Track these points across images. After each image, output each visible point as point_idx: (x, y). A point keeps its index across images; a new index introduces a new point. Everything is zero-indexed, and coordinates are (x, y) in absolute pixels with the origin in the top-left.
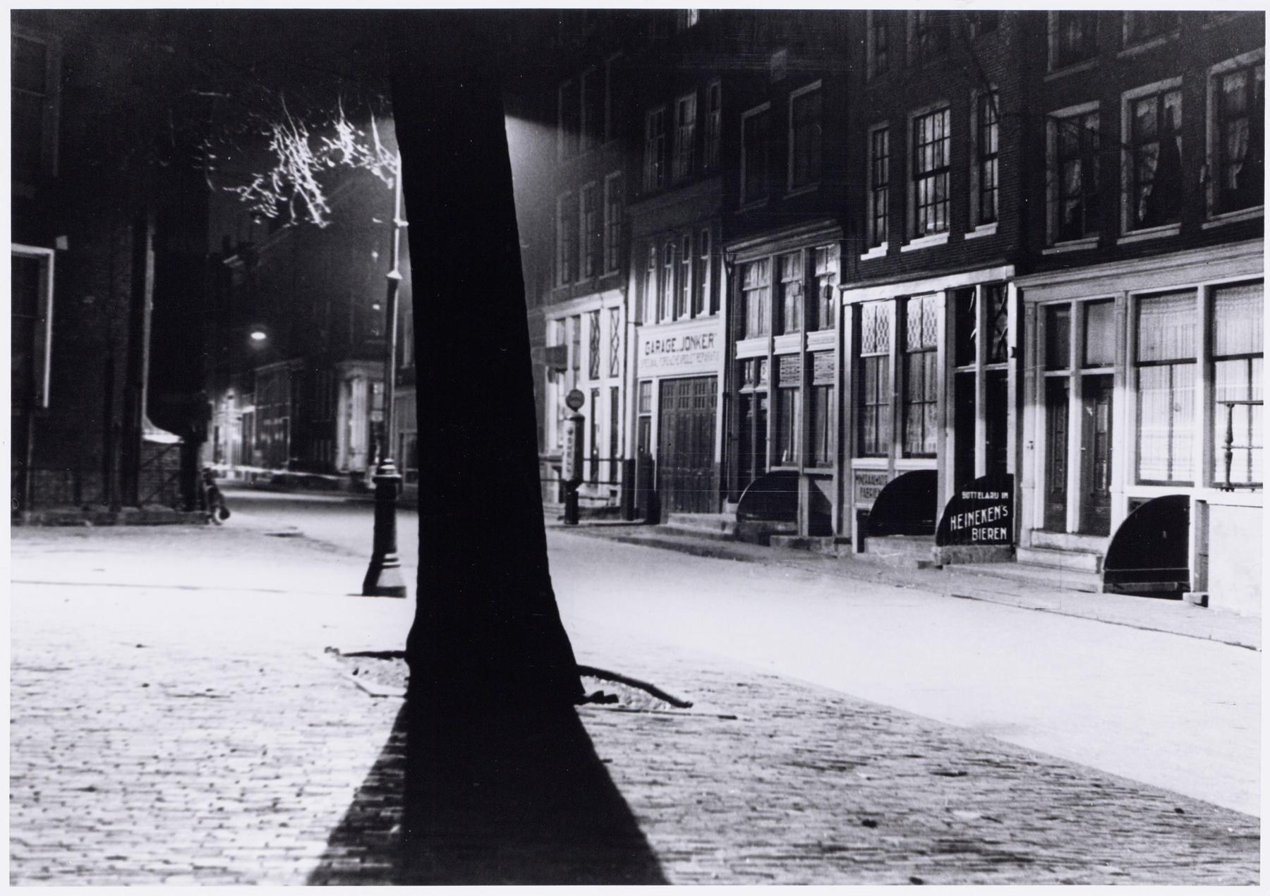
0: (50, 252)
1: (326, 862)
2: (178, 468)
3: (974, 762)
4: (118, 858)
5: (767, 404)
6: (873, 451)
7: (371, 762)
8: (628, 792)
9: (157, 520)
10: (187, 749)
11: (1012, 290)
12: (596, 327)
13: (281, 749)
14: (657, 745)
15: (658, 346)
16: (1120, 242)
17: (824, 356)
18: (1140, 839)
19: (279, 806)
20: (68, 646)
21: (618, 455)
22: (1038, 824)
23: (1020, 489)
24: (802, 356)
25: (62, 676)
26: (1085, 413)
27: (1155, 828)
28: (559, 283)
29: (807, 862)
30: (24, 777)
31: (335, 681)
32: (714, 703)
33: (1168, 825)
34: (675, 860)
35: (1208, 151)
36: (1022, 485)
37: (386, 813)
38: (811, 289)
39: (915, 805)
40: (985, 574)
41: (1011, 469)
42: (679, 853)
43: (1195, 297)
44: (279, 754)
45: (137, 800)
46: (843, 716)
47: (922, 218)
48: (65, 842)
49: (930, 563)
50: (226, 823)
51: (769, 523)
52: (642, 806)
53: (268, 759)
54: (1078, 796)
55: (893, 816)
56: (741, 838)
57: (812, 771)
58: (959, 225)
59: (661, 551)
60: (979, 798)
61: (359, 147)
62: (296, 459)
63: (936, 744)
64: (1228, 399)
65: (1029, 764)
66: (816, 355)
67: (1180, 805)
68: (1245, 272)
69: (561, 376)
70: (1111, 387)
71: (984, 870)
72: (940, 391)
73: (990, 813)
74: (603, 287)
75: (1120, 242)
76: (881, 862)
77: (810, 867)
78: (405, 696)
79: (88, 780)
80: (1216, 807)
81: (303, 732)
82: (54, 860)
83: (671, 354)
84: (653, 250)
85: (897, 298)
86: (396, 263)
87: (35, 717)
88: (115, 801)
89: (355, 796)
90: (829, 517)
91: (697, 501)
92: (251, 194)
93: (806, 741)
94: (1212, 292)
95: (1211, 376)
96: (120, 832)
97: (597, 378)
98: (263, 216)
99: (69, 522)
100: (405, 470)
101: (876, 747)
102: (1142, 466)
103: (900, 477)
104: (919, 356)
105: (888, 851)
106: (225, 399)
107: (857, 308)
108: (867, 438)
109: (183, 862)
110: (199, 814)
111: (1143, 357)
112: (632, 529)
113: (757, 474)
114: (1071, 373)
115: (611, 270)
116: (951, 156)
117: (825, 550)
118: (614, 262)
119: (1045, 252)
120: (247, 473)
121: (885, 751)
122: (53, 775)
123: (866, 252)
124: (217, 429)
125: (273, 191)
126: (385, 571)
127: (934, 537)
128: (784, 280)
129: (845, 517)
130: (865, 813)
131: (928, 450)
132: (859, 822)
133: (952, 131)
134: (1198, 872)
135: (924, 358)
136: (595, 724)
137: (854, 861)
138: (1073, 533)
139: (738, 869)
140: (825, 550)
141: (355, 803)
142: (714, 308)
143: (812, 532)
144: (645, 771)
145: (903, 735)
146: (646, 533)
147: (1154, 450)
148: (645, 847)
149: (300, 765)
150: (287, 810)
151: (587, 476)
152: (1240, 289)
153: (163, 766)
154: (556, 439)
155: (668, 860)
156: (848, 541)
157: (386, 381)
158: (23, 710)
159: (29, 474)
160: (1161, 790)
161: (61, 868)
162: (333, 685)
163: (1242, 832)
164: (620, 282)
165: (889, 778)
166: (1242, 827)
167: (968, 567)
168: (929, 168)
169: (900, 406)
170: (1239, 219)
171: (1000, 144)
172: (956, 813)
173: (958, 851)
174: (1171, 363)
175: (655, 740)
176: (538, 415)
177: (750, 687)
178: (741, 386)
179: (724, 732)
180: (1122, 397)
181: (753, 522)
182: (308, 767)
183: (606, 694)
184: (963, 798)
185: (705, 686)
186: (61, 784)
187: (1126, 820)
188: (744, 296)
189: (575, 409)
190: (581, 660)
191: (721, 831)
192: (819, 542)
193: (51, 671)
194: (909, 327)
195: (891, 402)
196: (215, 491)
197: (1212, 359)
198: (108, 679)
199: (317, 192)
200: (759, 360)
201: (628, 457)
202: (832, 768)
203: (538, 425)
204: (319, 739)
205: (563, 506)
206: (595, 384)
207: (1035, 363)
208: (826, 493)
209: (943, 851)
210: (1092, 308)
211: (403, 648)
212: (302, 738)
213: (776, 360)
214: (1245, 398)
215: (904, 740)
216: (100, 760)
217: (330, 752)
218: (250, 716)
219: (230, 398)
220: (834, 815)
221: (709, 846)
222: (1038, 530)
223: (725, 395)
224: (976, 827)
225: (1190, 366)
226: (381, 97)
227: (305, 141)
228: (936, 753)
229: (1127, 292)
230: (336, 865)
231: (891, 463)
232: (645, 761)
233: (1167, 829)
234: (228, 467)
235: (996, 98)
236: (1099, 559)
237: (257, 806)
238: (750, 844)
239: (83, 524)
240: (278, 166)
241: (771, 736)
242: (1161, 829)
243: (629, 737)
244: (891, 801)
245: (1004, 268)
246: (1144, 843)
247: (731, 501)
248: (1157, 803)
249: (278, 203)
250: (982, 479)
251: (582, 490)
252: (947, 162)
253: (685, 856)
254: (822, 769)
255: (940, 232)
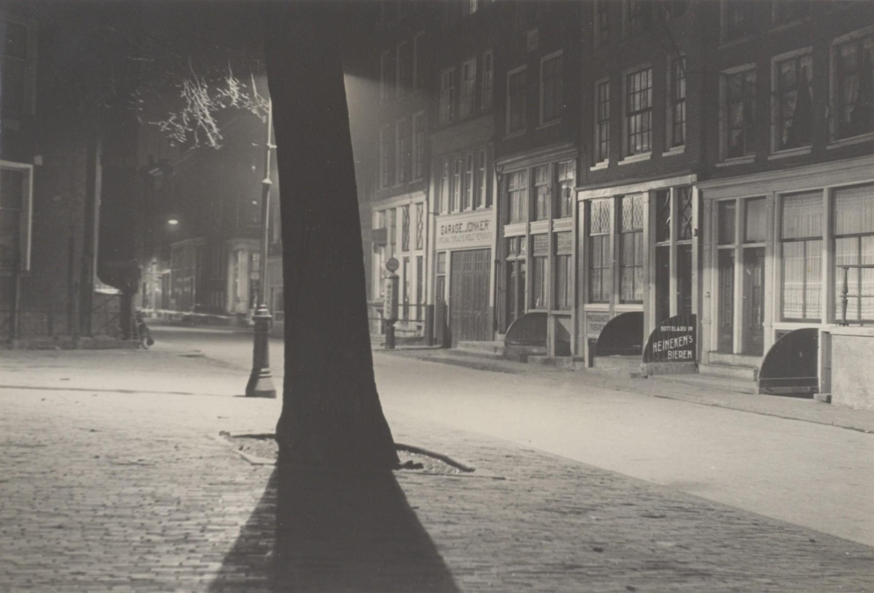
0: (30, 166)
1: (221, 576)
2: (118, 311)
3: (671, 509)
4: (79, 573)
5: (525, 267)
6: (599, 299)
7: (252, 509)
8: (431, 528)
9: (104, 346)
10: (125, 500)
11: (695, 191)
12: (406, 216)
13: (190, 500)
14: (451, 497)
15: (450, 229)
16: (770, 158)
17: (564, 235)
18: (785, 560)
19: (189, 538)
20: (44, 430)
21: (423, 302)
22: (715, 550)
23: (701, 325)
24: (549, 236)
25: (41, 451)
26: (745, 273)
27: (795, 553)
28: (381, 187)
29: (554, 575)
30: (14, 518)
31: (227, 454)
32: (490, 469)
33: (805, 550)
34: (463, 574)
35: (831, 97)
36: (703, 322)
37: (263, 543)
38: (556, 191)
39: (630, 537)
40: (677, 381)
41: (694, 311)
42: (465, 569)
43: (822, 196)
44: (188, 503)
45: (91, 535)
46: (579, 477)
47: (633, 142)
48: (43, 562)
49: (639, 374)
50: (153, 550)
51: (527, 347)
52: (441, 538)
53: (181, 507)
54: (742, 531)
55: (614, 544)
56: (509, 559)
57: (557, 515)
58: (658, 147)
59: (452, 366)
60: (674, 533)
61: (243, 95)
62: (199, 305)
63: (644, 496)
64: (844, 264)
65: (709, 510)
66: (559, 235)
67: (813, 537)
68: (857, 179)
69: (383, 249)
70: (763, 256)
71: (678, 582)
72: (645, 259)
73: (681, 543)
74: (412, 189)
75: (770, 158)
76: (606, 576)
77: (557, 579)
78: (276, 464)
79: (58, 521)
80: (838, 538)
81: (205, 489)
82: (35, 575)
83: (459, 234)
84: (447, 164)
85: (615, 196)
86: (268, 173)
87: (22, 478)
88: (77, 535)
89: (241, 532)
90: (569, 344)
91: (477, 331)
92: (168, 126)
93: (553, 494)
94: (833, 192)
95: (832, 249)
96: (80, 556)
97: (408, 250)
98: (176, 141)
99: (44, 347)
100: (275, 312)
101: (602, 498)
102: (848, 310)
103: (618, 317)
104: (630, 235)
105: (611, 568)
106: (150, 265)
107: (588, 203)
108: (595, 290)
109: (123, 576)
110: (134, 544)
111: (786, 236)
112: (431, 352)
113: (519, 315)
114: (736, 247)
115: (417, 178)
116: (653, 100)
117: (566, 366)
118: (419, 173)
119: (718, 165)
120: (165, 314)
121: (609, 501)
122: (34, 517)
123: (594, 165)
124: (145, 285)
125: (183, 124)
126: (261, 380)
127: (642, 357)
128: (537, 184)
129: (580, 343)
130: (596, 543)
131: (637, 298)
132: (591, 549)
133: (653, 83)
134: (825, 582)
135: (634, 236)
136: (407, 483)
137: (588, 575)
138: (738, 354)
139: (507, 580)
140: (566, 366)
141: (241, 537)
142: (489, 203)
143: (557, 353)
144: (442, 514)
145: (621, 490)
146: (442, 354)
147: (793, 297)
148: (443, 565)
149: (203, 511)
150: (195, 541)
151: (401, 316)
152: (853, 190)
153: (108, 512)
154: (379, 291)
155: (458, 574)
156: (582, 360)
157: (261, 252)
158: (14, 474)
159: (17, 315)
160: (799, 527)
161: (39, 580)
162: (225, 457)
163: (855, 555)
164: (423, 186)
165: (612, 519)
166: (855, 551)
167: (666, 377)
168: (638, 108)
169: (617, 268)
170: (852, 143)
171: (687, 92)
172: (659, 543)
173: (660, 568)
174: (805, 240)
175: (448, 493)
176: (366, 275)
177: (514, 457)
178: (508, 256)
179: (496, 488)
180: (771, 264)
181: (516, 348)
182: (209, 512)
183: (414, 463)
184: (662, 533)
185: (484, 457)
186: (40, 523)
187: (776, 548)
188: (510, 195)
189: (393, 271)
190: (397, 440)
191: (495, 555)
192: (562, 360)
193: (33, 447)
194: (624, 215)
195: (611, 266)
196: (143, 327)
197: (833, 237)
198: (71, 452)
199: (214, 125)
200: (521, 237)
201: (429, 303)
202: (571, 512)
203: (367, 281)
204: (216, 494)
205: (384, 336)
206: (406, 254)
207: (711, 240)
208: (567, 328)
209: (649, 569)
210: (750, 203)
211: (274, 432)
212: (204, 493)
213: (532, 238)
214: (857, 264)
215: (622, 493)
216: (66, 507)
217: (223, 502)
218: (168, 478)
219: (154, 263)
220: (573, 544)
221: (487, 564)
222: (714, 352)
223: (497, 262)
224: (673, 552)
225: (818, 242)
226: (258, 61)
227: (205, 90)
228: (644, 502)
229: (774, 192)
230: (229, 578)
231: (612, 307)
232: (442, 508)
233: (804, 553)
234: (152, 310)
235: (684, 61)
236: (756, 372)
237: (173, 538)
238: (515, 563)
239: (54, 349)
240: (186, 107)
241: (529, 491)
242: (799, 553)
243: (430, 491)
244: (613, 534)
245: (690, 176)
246: (788, 563)
247: (501, 333)
248: (797, 536)
249: (187, 133)
250: (675, 318)
251: (397, 325)
252: (650, 104)
253: (470, 571)
254: (565, 513)
255: (646, 151)
